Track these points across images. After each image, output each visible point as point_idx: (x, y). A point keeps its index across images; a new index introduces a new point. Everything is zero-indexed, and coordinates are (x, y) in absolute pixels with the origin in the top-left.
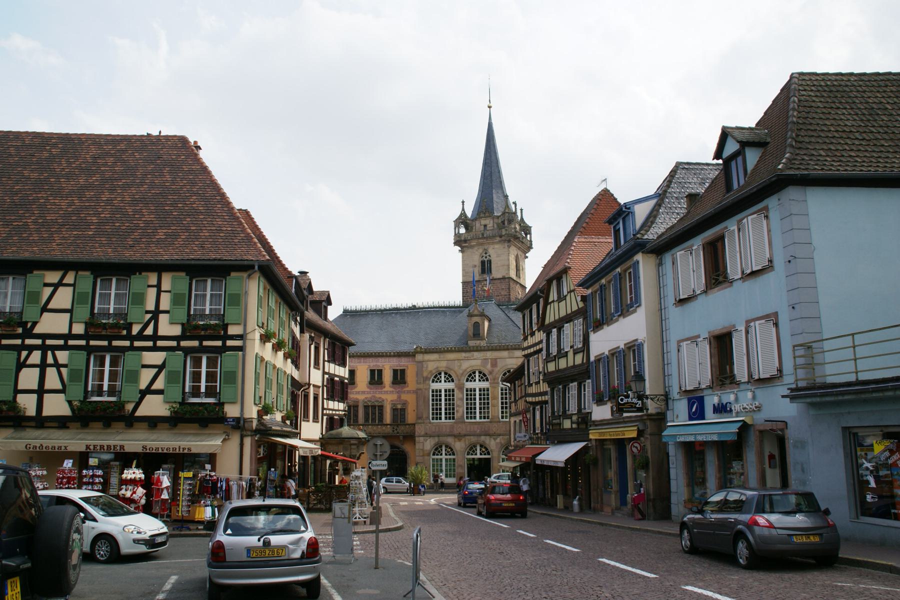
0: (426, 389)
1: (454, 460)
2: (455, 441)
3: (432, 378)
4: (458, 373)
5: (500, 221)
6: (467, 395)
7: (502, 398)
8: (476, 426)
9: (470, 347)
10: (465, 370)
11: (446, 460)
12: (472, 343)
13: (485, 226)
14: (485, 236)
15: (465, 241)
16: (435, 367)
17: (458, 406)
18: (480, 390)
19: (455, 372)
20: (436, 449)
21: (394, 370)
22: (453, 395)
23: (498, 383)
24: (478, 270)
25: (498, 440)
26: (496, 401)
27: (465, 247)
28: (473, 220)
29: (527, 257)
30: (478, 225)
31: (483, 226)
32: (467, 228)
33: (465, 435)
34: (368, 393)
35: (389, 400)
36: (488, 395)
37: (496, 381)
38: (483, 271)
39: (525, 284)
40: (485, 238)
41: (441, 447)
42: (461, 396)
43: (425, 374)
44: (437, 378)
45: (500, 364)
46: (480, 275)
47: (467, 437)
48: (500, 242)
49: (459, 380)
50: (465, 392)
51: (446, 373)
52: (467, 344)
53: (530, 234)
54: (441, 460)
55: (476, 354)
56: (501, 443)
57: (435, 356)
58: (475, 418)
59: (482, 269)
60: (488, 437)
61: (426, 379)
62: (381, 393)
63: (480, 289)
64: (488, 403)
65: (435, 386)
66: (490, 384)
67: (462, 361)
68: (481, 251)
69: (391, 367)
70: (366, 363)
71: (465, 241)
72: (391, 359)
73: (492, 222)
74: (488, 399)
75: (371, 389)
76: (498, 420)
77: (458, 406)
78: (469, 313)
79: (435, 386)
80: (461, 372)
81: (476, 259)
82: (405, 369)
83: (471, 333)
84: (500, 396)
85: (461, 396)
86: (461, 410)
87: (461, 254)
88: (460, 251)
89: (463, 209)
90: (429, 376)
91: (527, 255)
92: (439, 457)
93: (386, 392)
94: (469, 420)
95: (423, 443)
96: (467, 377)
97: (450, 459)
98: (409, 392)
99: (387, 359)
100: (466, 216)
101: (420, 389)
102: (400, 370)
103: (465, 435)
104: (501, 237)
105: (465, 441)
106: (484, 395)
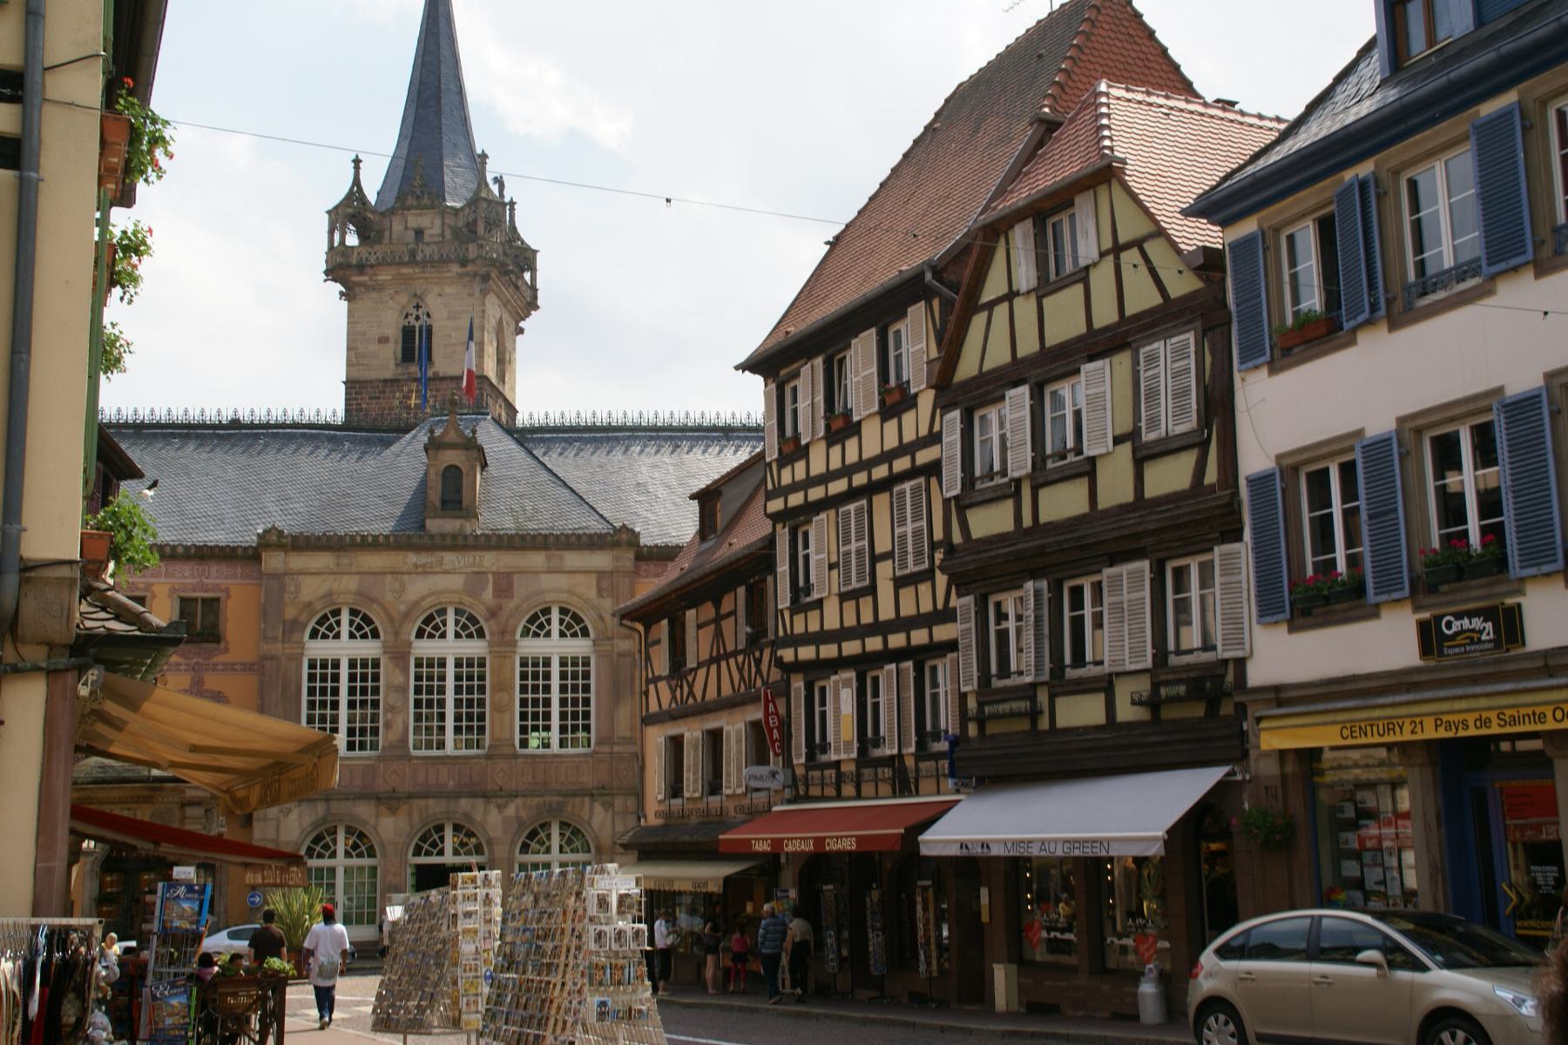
0: (291, 658)
1: (373, 869)
2: (378, 815)
3: (312, 624)
5: (461, 223)
6: (418, 677)
7: (524, 689)
8: (444, 771)
9: (432, 537)
10: (417, 603)
11: (347, 870)
12: (434, 525)
13: (419, 233)
14: (419, 258)
15: (361, 267)
16: (322, 591)
17: (391, 709)
18: (458, 664)
19: (383, 607)
20: (317, 840)
21: (183, 600)
22: (376, 678)
23: (514, 644)
24: (392, 351)
25: (510, 810)
26: (505, 696)
27: (359, 284)
28: (382, 214)
29: (521, 331)
30: (397, 227)
31: (412, 233)
32: (362, 235)
33: (411, 796)
36: (482, 677)
37: (508, 637)
38: (408, 355)
39: (514, 401)
40: (418, 263)
41: (333, 832)
42: (398, 679)
43: (290, 613)
44: (326, 627)
45: (521, 587)
46: (397, 365)
47: (416, 802)
48: (461, 276)
49: (397, 633)
50: (412, 670)
51: (354, 612)
52: (422, 527)
53: (533, 270)
54: (332, 871)
55: (450, 558)
56: (518, 818)
57: (323, 560)
58: (441, 745)
59: (404, 349)
60: (480, 802)
61: (294, 626)
63: (397, 402)
64: (481, 703)
65: (320, 649)
66: (491, 645)
67: (406, 577)
68: (403, 299)
69: (173, 590)
71: (361, 267)
73: (438, 222)
74: (482, 689)
76: (507, 750)
77: (391, 709)
78: (431, 439)
79: (320, 649)
80: (403, 608)
81: (390, 322)
82: (217, 600)
83: (435, 495)
84: (518, 682)
85: (398, 679)
86: (399, 720)
87: (344, 304)
88: (342, 294)
89: (357, 181)
90: (303, 618)
91: (522, 324)
92: (326, 863)
94: (424, 752)
95: (278, 821)
96: (418, 623)
97: (361, 869)
98: (230, 668)
100: (362, 198)
101: (273, 658)
102: (204, 600)
103: (411, 796)
104: (464, 262)
105: (410, 814)
106: (470, 678)
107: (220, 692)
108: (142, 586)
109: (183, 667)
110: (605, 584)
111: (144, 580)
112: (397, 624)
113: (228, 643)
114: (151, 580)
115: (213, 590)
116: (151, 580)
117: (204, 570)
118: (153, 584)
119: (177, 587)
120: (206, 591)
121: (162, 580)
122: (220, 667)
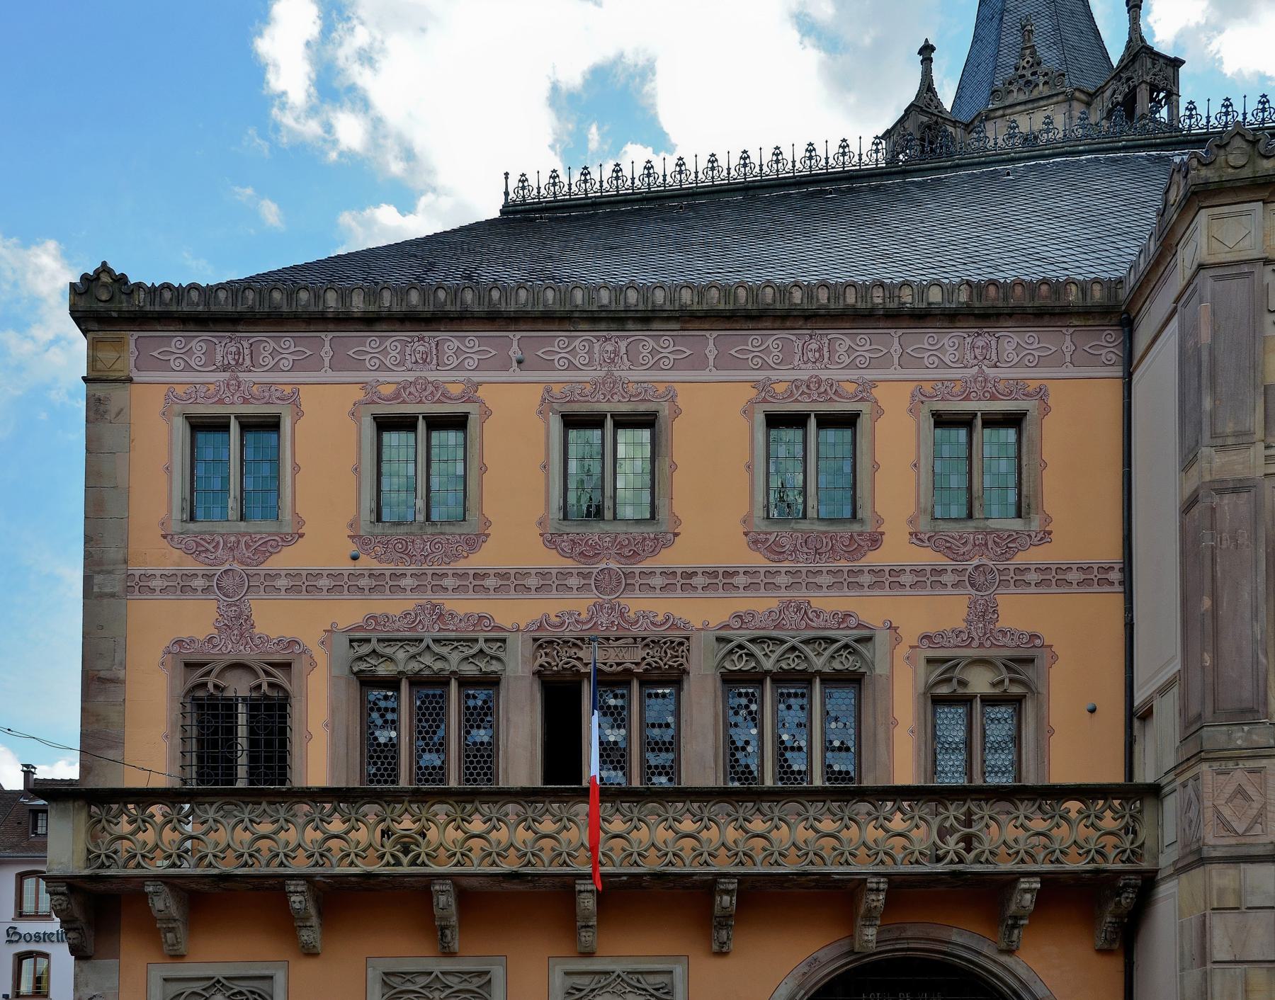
34: (757, 581)
35: (910, 634)
62: (850, 580)
69: (920, 397)
70: (738, 364)
72: (926, 340)
75: (775, 551)
93: (889, 579)
99: (894, 340)
107: (1034, 636)
108: (851, 388)
109: (948, 578)
111: (853, 374)
113: (1048, 519)
114: (870, 375)
115: (1009, 395)
116: (870, 375)
117: (987, 347)
118: (874, 384)
119: (927, 388)
120: (993, 398)
121: (895, 372)
122: (1033, 577)
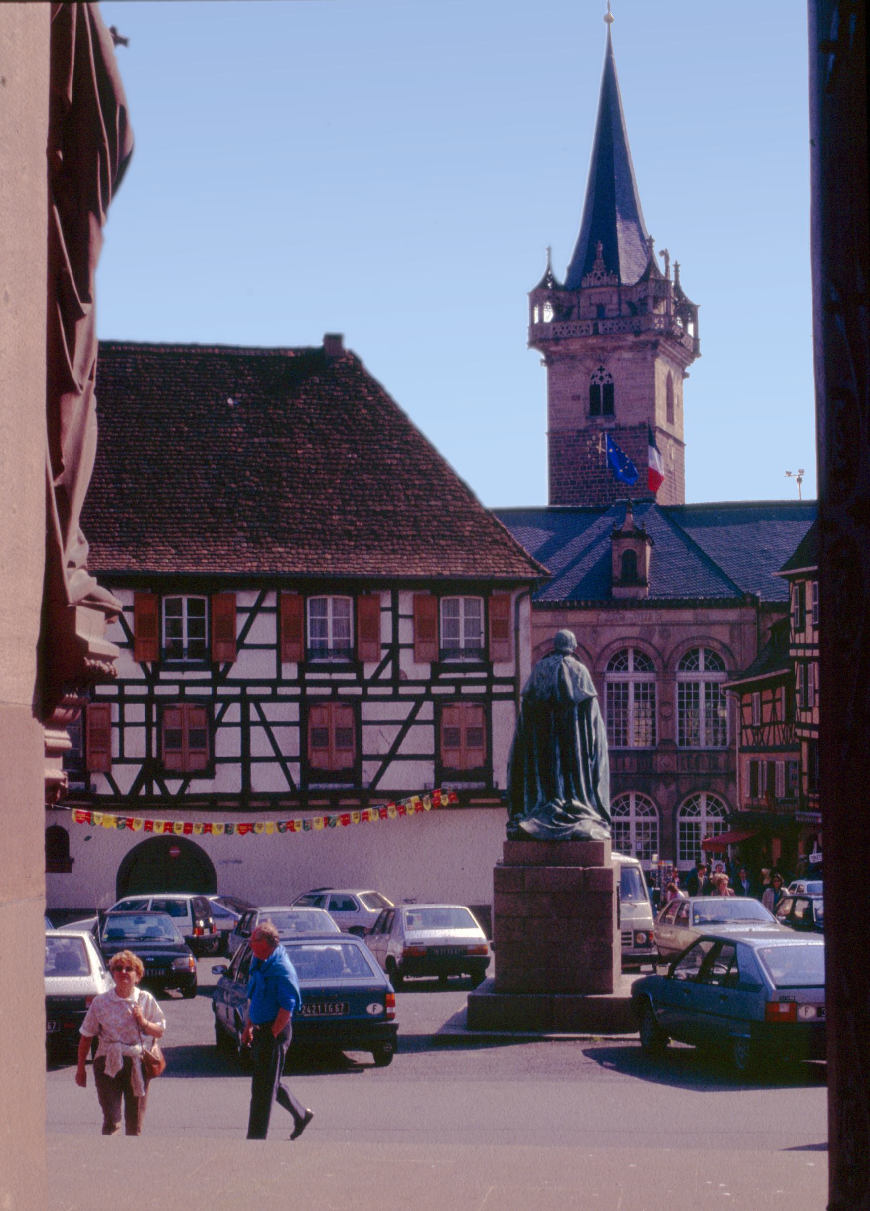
4: (592, 653)
24: (580, 408)
31: (594, 309)
46: (587, 418)
53: (695, 321)
55: (629, 615)
59: (592, 405)
80: (598, 650)
81: (580, 383)
84: (677, 700)
88: (542, 361)
110: (736, 633)
112: (595, 661)
